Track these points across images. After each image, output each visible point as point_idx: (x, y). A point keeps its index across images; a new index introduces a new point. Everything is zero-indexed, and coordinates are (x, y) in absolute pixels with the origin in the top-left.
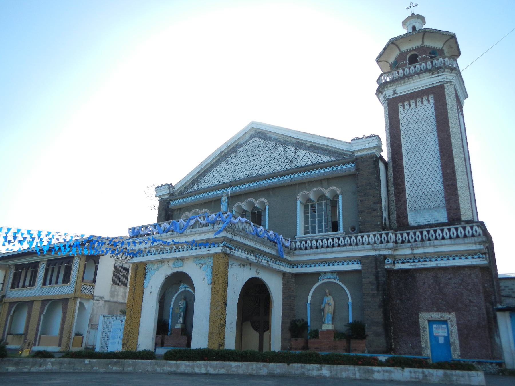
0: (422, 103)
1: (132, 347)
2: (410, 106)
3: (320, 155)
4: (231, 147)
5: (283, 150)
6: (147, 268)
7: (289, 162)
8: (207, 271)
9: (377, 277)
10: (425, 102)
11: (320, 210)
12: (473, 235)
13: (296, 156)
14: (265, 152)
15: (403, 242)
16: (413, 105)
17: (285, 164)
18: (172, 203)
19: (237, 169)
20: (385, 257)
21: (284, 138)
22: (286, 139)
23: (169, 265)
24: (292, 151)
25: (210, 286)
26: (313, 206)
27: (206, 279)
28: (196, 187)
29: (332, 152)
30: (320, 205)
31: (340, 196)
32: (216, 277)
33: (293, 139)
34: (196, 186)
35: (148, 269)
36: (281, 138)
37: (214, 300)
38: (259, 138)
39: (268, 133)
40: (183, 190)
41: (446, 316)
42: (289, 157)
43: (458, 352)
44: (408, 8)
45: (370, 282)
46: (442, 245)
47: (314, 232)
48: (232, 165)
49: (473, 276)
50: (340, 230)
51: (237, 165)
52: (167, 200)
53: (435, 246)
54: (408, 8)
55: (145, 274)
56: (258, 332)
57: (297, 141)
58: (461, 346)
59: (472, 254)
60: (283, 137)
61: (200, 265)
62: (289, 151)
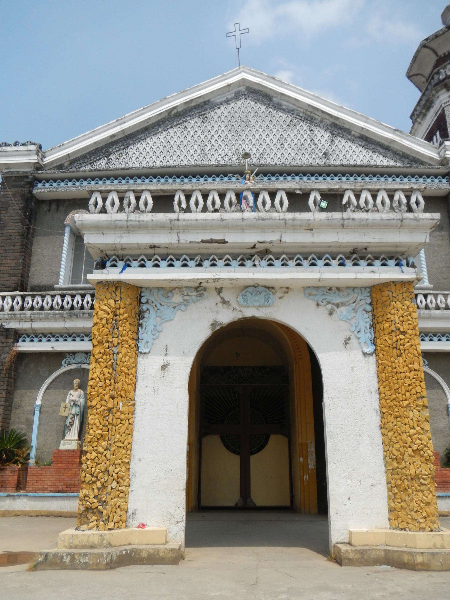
1: (115, 520)
3: (377, 154)
4: (193, 104)
5: (309, 133)
6: (143, 300)
7: (321, 155)
8: (354, 321)
13: (334, 147)
14: (271, 127)
17: (314, 156)
19: (209, 146)
21: (309, 113)
22: (312, 115)
23: (222, 298)
25: (373, 359)
27: (354, 341)
28: (103, 164)
29: (399, 155)
32: (402, 336)
33: (327, 117)
35: (147, 303)
36: (302, 110)
37: (408, 394)
38: (256, 101)
39: (275, 95)
40: (66, 164)
42: (320, 146)
48: (196, 137)
51: (209, 138)
52: (27, 177)
55: (140, 315)
56: (237, 454)
57: (333, 123)
60: (307, 110)
61: (330, 306)
62: (319, 137)
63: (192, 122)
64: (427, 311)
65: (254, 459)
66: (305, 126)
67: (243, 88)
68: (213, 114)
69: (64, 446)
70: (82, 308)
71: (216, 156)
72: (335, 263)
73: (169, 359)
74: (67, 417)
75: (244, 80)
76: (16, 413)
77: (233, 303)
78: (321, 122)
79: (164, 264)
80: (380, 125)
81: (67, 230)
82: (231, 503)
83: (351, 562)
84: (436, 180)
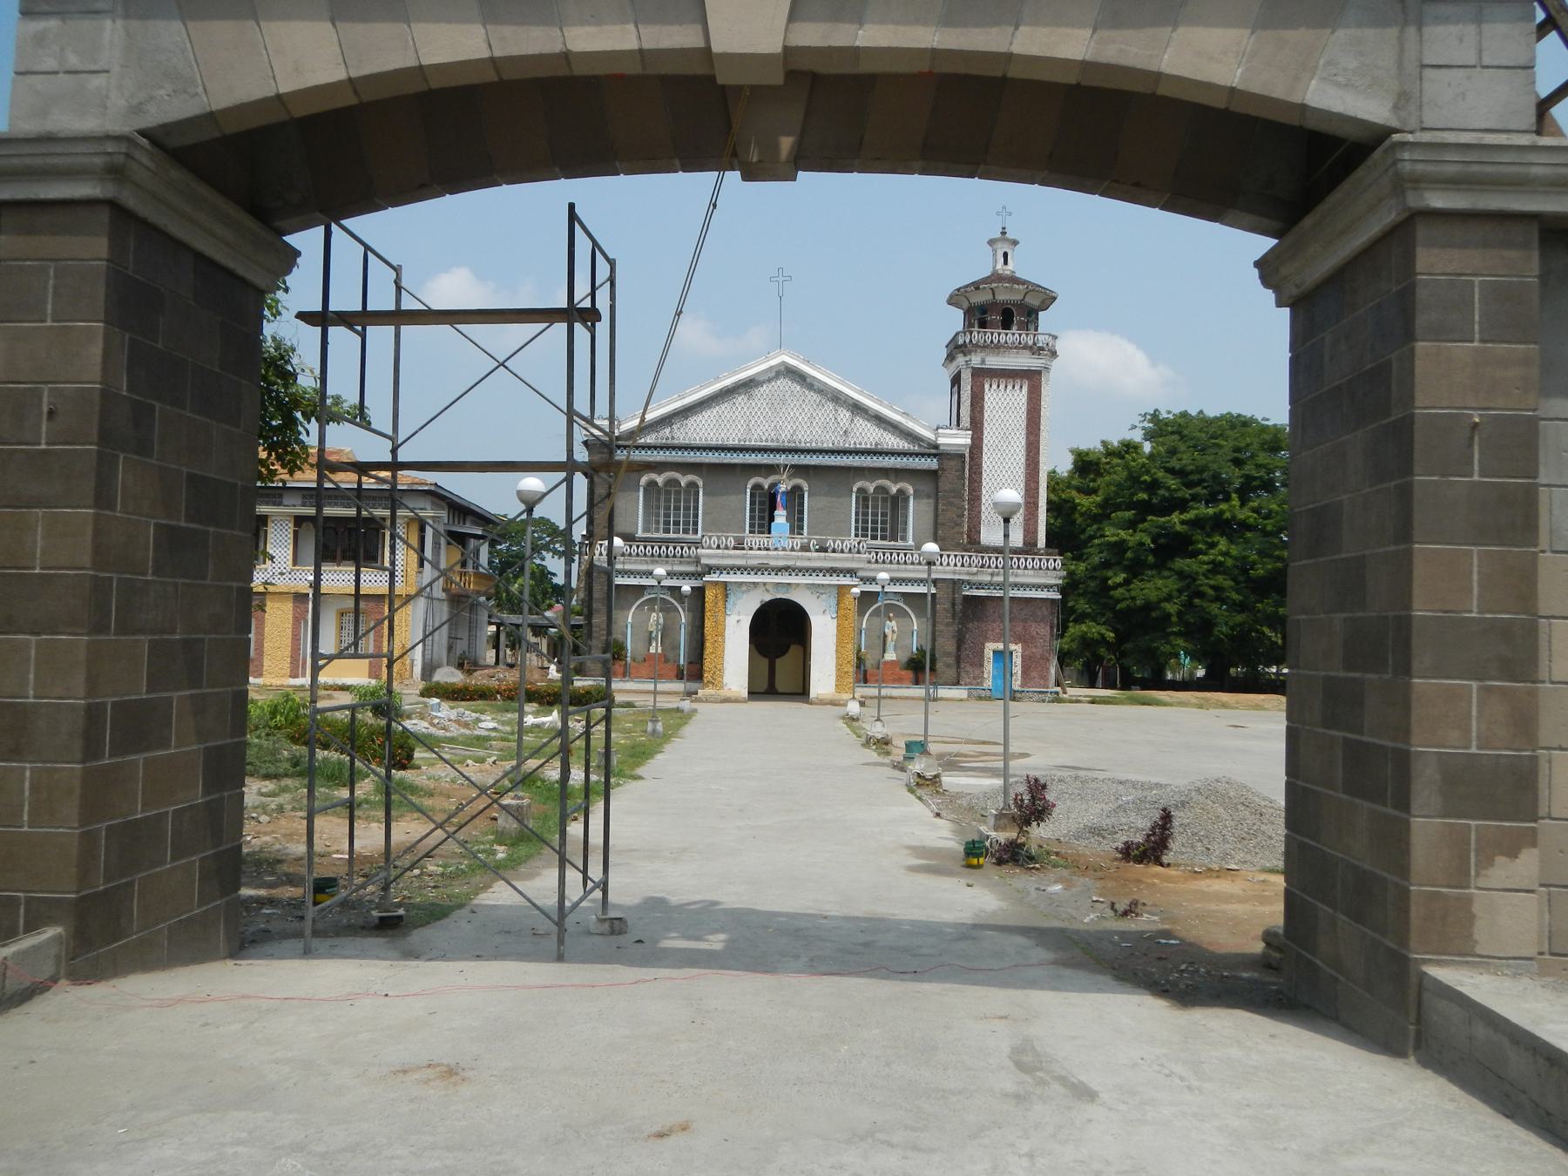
0: (1014, 387)
2: (998, 386)
9: (953, 604)
10: (1017, 387)
11: (875, 507)
12: (1055, 569)
15: (983, 566)
16: (1002, 387)
18: (619, 452)
20: (963, 581)
24: (847, 415)
26: (866, 499)
27: (828, 612)
30: (875, 500)
31: (911, 498)
34: (667, 431)
38: (793, 380)
41: (1012, 647)
43: (1019, 682)
44: (998, 214)
45: (945, 609)
46: (1024, 575)
47: (874, 538)
49: (1044, 609)
50: (904, 538)
53: (1016, 576)
54: (998, 214)
55: (727, 596)
58: (1022, 677)
59: (1049, 587)
63: (740, 399)
64: (904, 566)
65: (778, 662)
66: (831, 405)
67: (782, 368)
68: (756, 391)
69: (652, 650)
70: (660, 556)
71: (759, 431)
72: (821, 575)
73: (741, 617)
74: (651, 632)
75: (784, 363)
76: (615, 627)
77: (771, 590)
78: (845, 402)
79: (739, 572)
80: (891, 408)
81: (641, 489)
82: (761, 690)
83: (816, 704)
84: (929, 460)
